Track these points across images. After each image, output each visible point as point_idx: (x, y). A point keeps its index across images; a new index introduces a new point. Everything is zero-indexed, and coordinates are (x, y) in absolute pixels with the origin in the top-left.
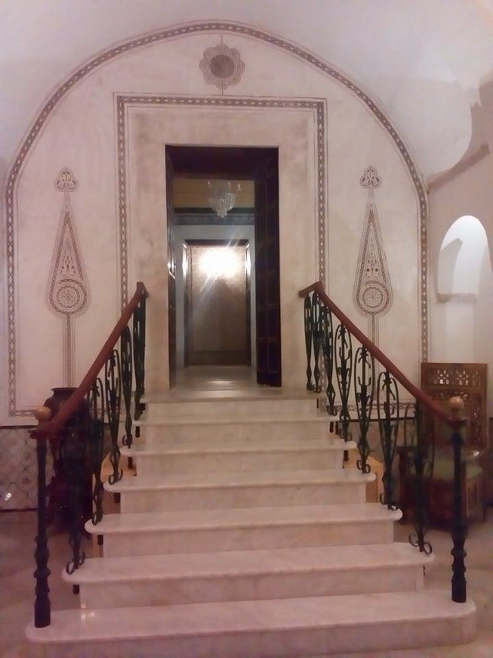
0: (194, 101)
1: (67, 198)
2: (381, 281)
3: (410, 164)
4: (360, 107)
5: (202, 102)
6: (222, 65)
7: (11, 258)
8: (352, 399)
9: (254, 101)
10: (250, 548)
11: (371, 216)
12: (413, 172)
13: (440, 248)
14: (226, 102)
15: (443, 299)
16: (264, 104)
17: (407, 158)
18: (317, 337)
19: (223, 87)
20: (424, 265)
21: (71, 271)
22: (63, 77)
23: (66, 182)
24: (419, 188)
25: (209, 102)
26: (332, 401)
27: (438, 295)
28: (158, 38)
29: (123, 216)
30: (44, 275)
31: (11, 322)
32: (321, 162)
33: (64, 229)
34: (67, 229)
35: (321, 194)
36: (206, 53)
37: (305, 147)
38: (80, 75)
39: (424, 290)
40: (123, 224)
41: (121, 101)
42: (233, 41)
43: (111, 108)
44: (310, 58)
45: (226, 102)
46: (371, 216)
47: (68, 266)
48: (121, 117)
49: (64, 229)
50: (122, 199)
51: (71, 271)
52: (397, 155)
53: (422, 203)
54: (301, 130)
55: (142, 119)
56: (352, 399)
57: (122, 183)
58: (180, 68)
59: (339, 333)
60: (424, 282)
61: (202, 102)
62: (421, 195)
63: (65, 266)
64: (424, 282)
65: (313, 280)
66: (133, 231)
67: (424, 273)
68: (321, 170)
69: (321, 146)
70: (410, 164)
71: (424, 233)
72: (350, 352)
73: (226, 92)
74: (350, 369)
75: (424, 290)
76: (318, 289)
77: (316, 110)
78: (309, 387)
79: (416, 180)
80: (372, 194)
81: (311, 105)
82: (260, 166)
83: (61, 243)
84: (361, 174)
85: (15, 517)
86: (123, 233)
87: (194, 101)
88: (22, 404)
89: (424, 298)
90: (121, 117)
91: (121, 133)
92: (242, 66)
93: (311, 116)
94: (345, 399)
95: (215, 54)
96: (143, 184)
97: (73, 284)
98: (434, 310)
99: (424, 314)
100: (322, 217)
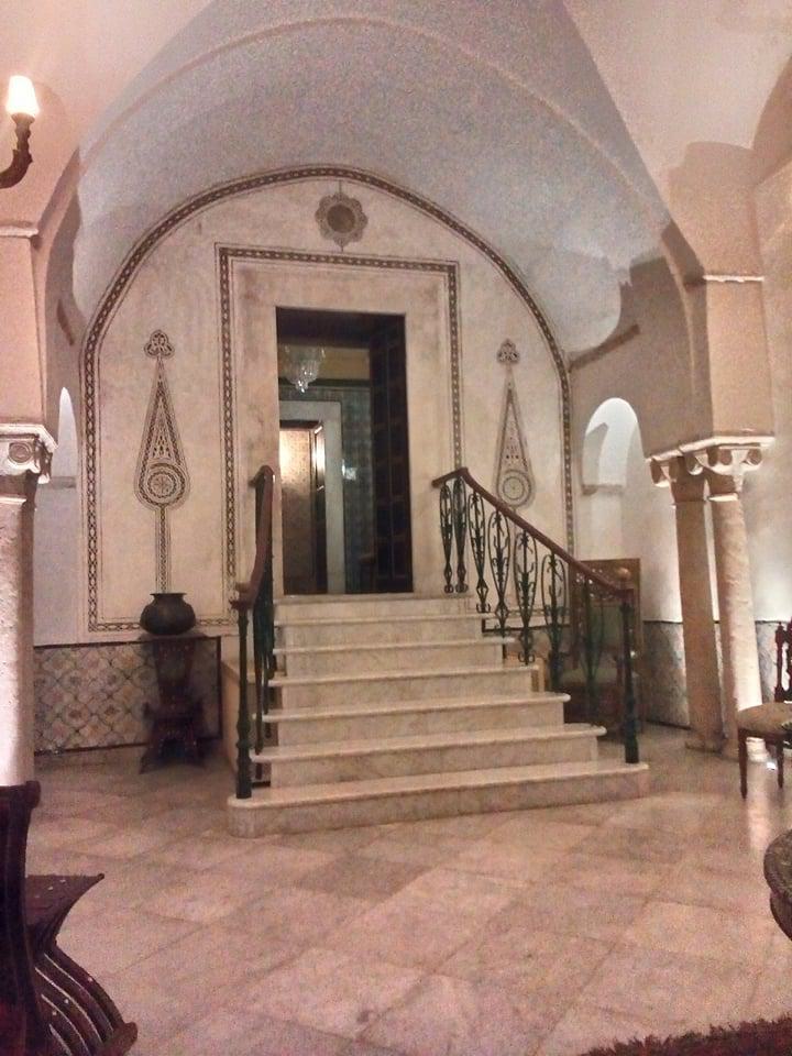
0: (309, 258)
1: (161, 365)
2: (522, 468)
3: (551, 339)
4: (495, 273)
5: (318, 259)
6: (341, 218)
7: (91, 437)
8: (510, 589)
9: (378, 261)
10: (427, 733)
11: (510, 396)
12: (553, 348)
13: (585, 429)
14: (346, 261)
15: (588, 491)
16: (389, 264)
17: (547, 332)
18: (454, 527)
19: (342, 243)
20: (567, 452)
21: (166, 454)
22: (153, 220)
23: (159, 346)
24: (560, 365)
25: (327, 259)
26: (483, 598)
27: (583, 486)
28: (267, 182)
29: (227, 389)
30: (132, 459)
31: (91, 515)
32: (454, 333)
33: (157, 403)
34: (161, 403)
35: (455, 369)
36: (323, 203)
37: (436, 315)
38: (173, 220)
39: (568, 480)
40: (228, 399)
41: (224, 254)
42: (353, 190)
43: (212, 260)
44: (440, 215)
45: (346, 261)
46: (510, 396)
47: (161, 448)
48: (224, 272)
49: (157, 403)
50: (227, 369)
51: (166, 454)
52: (536, 331)
53: (564, 383)
54: (431, 294)
55: (248, 275)
56: (510, 589)
57: (227, 350)
58: (290, 216)
59: (493, 521)
60: (568, 471)
61: (318, 259)
62: (562, 374)
63: (158, 447)
64: (568, 471)
65: (449, 468)
66: (239, 407)
67: (568, 462)
68: (454, 343)
69: (453, 315)
70: (551, 339)
71: (566, 417)
72: (508, 540)
73: (346, 249)
74: (508, 559)
75: (568, 480)
76: (461, 474)
77: (447, 274)
78: (448, 588)
79: (557, 357)
80: (510, 371)
81: (441, 268)
82: (382, 338)
83: (153, 420)
84: (498, 348)
85: (94, 757)
86: (228, 409)
87: (309, 258)
88: (107, 614)
89: (569, 490)
90: (224, 272)
91: (225, 291)
92: (364, 220)
93: (441, 279)
94: (501, 594)
95: (333, 203)
96: (252, 352)
97: (167, 470)
98: (580, 504)
99: (569, 508)
100: (456, 396)
